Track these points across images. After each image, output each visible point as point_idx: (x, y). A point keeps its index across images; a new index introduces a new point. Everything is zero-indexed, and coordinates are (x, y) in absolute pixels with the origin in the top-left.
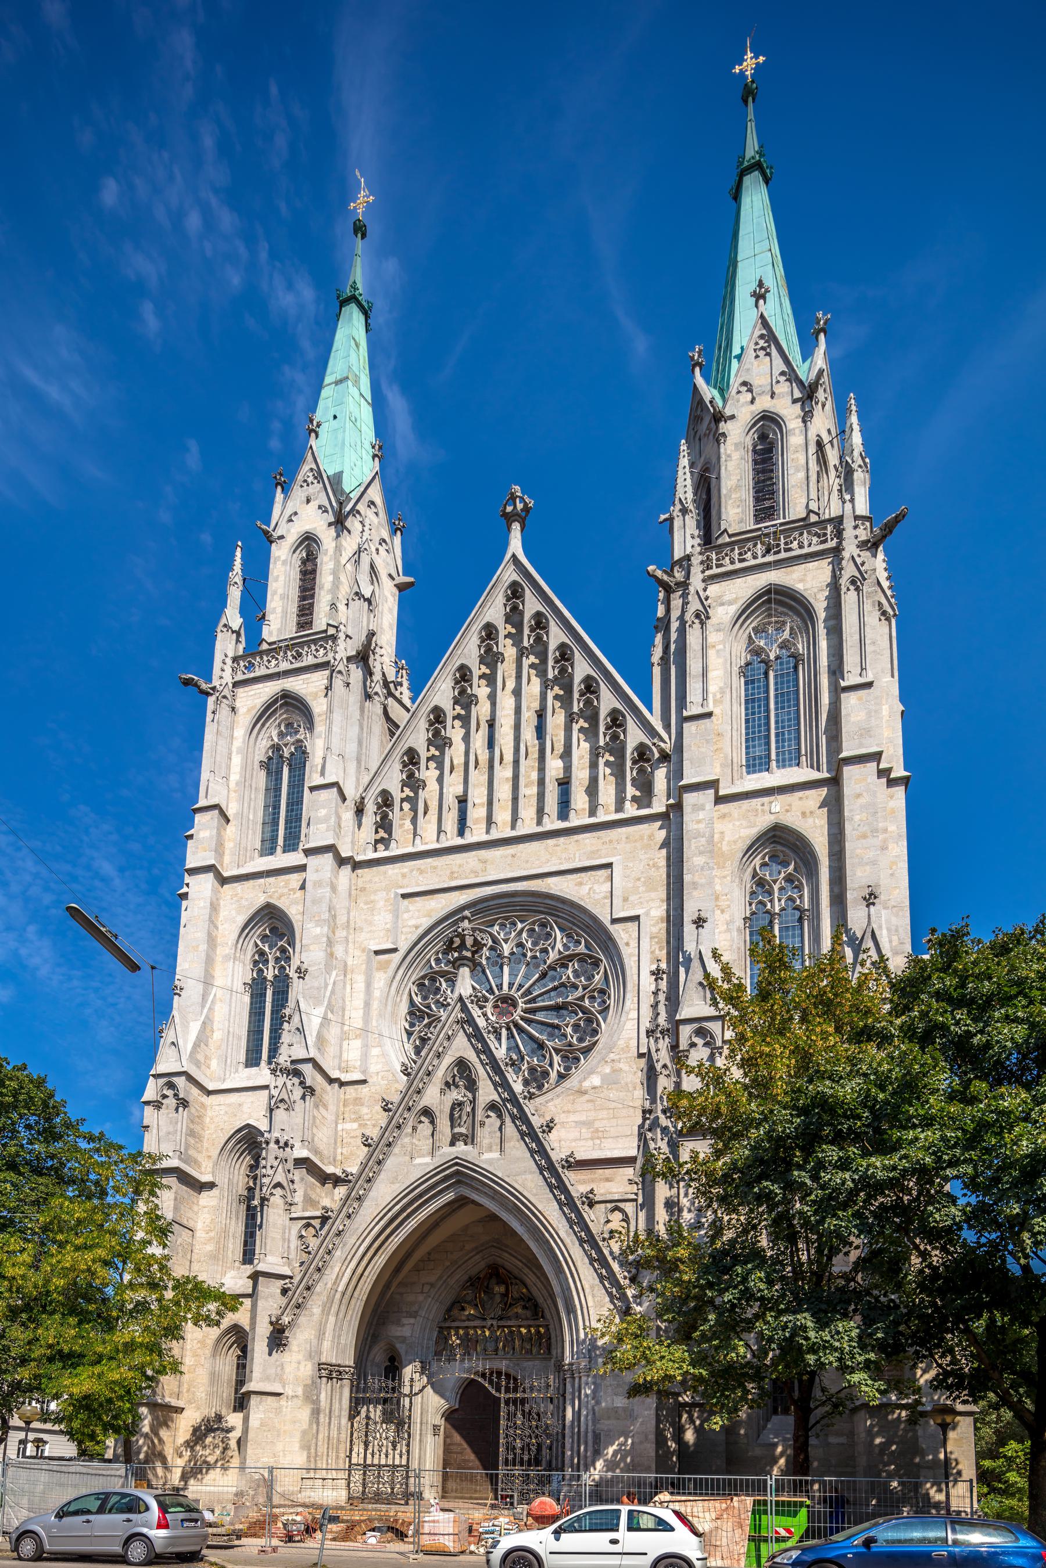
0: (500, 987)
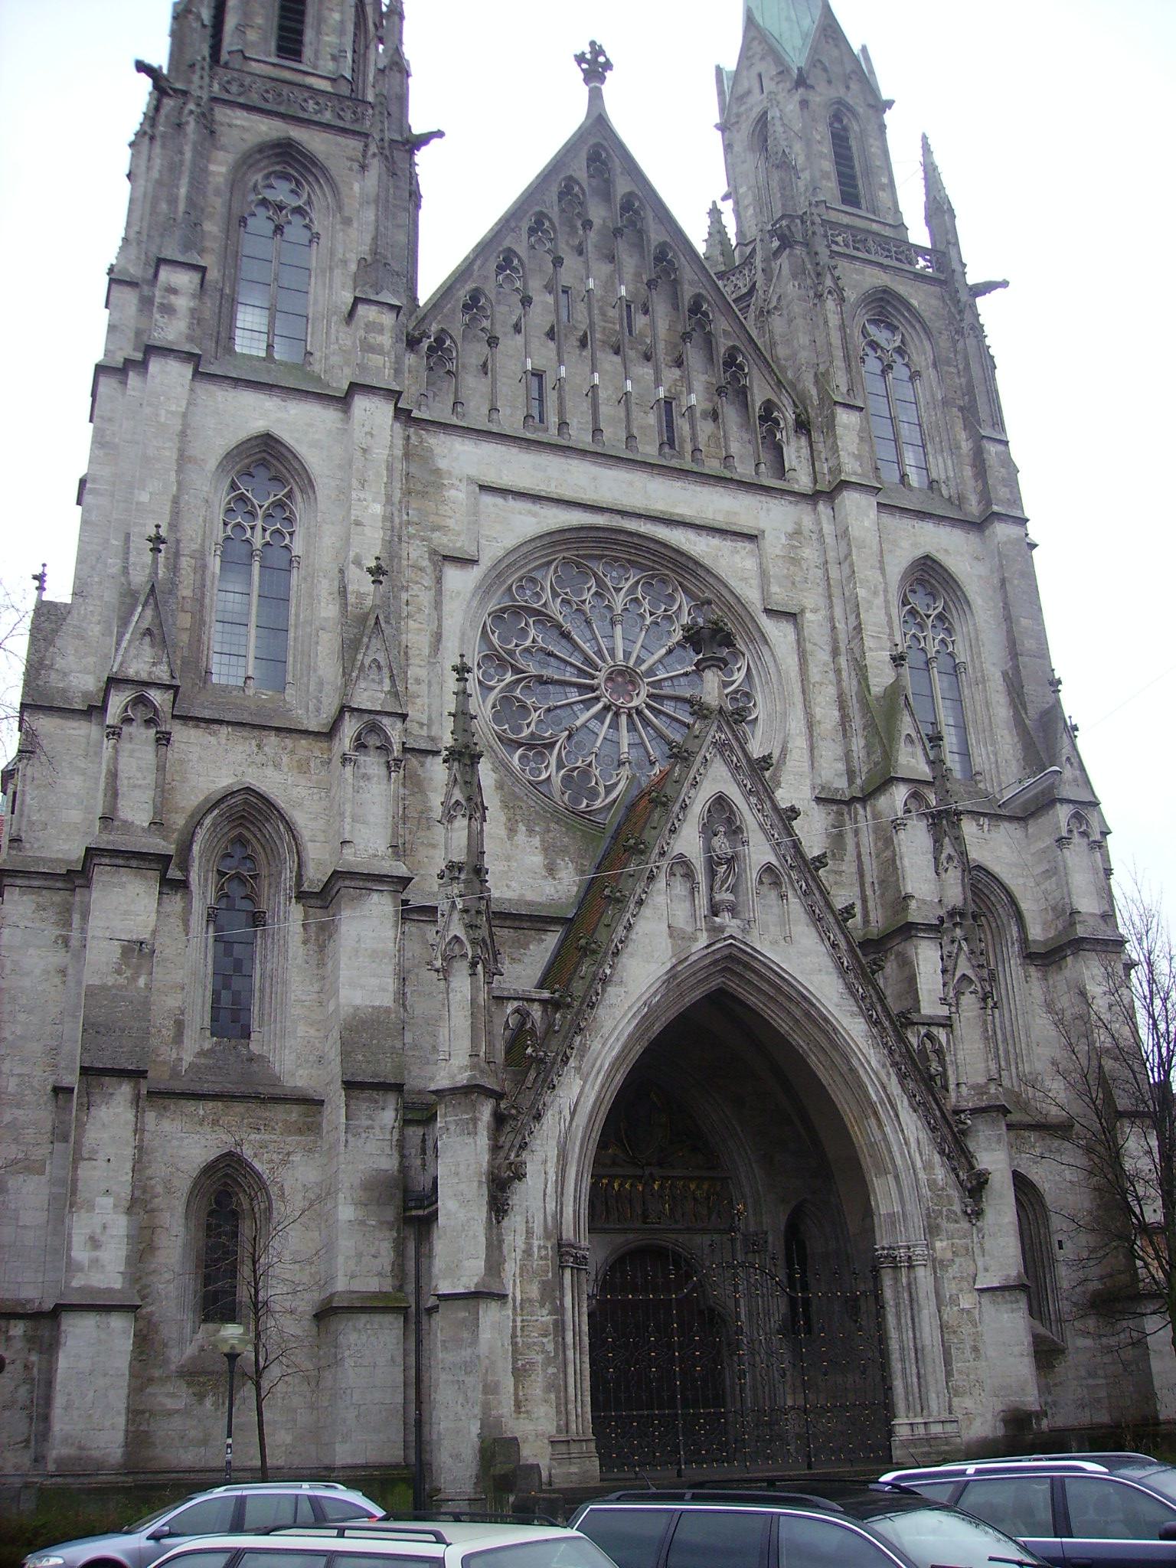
0: (612, 652)
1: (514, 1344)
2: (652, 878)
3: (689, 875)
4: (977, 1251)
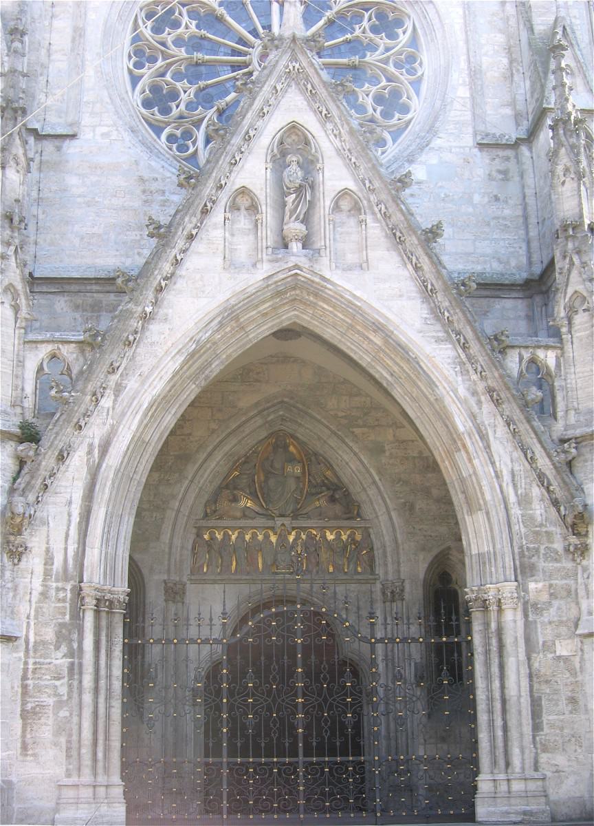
1: (24, 687)
2: (205, 212)
3: (254, 208)
4: (582, 593)
